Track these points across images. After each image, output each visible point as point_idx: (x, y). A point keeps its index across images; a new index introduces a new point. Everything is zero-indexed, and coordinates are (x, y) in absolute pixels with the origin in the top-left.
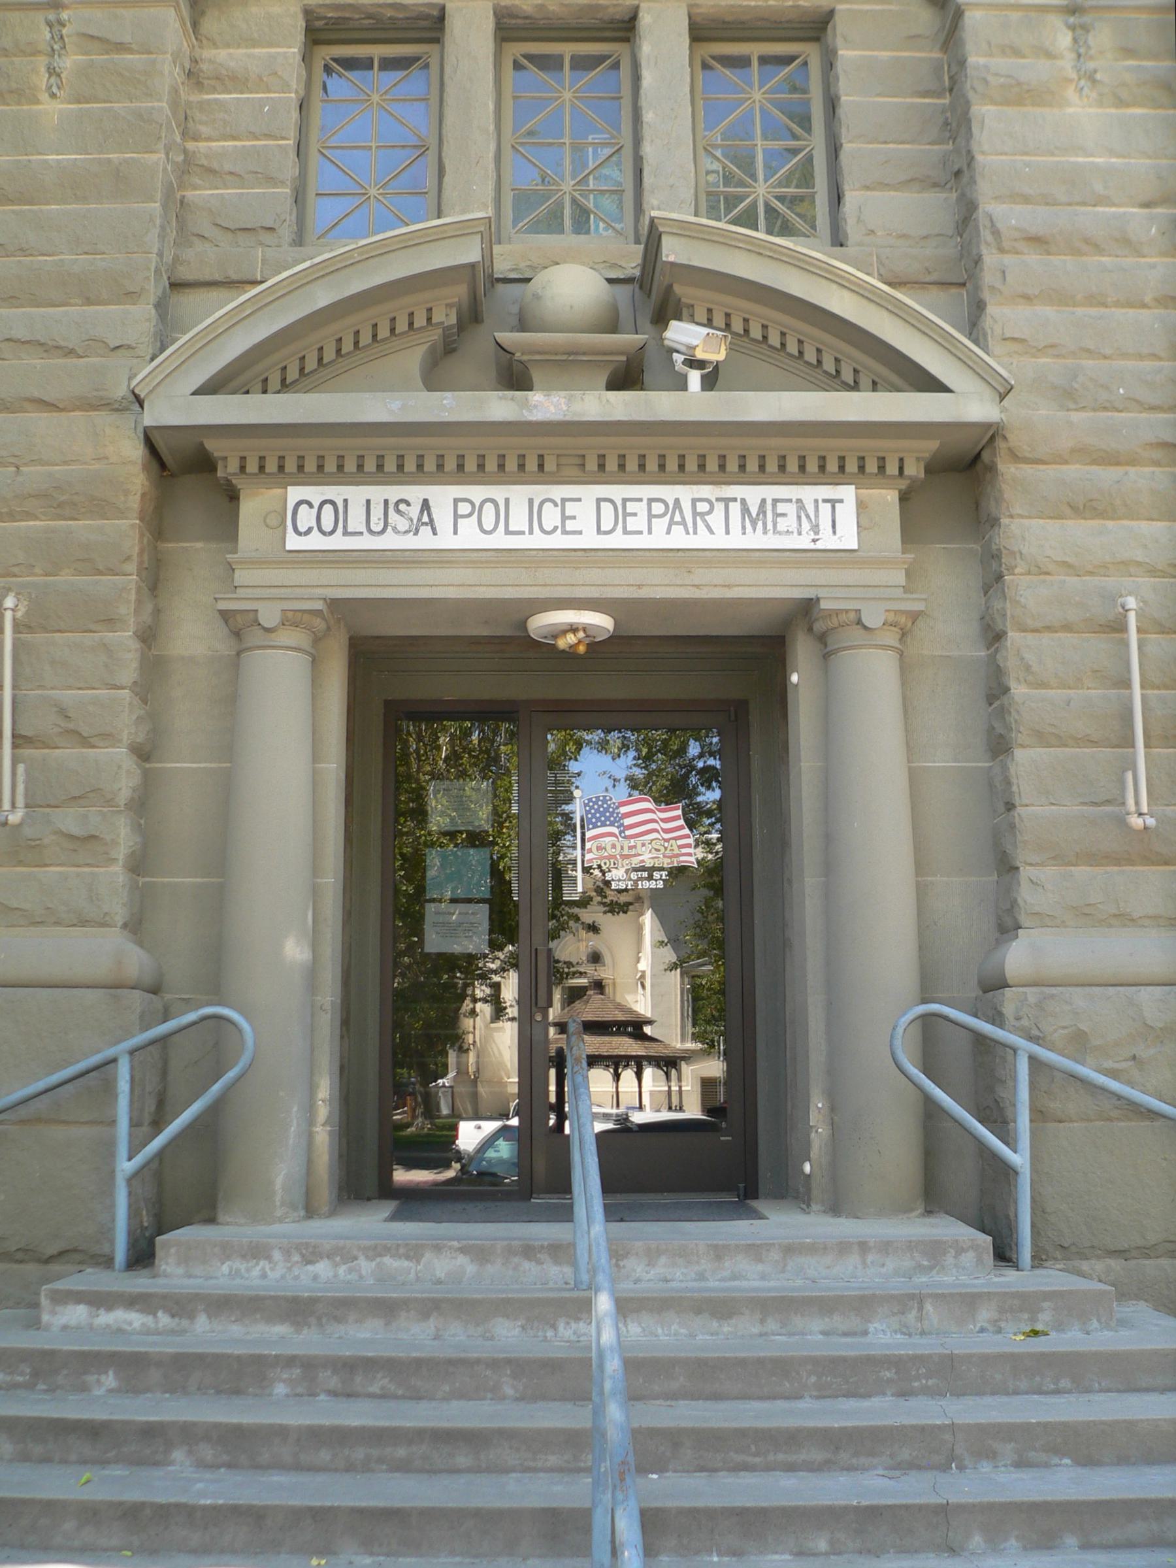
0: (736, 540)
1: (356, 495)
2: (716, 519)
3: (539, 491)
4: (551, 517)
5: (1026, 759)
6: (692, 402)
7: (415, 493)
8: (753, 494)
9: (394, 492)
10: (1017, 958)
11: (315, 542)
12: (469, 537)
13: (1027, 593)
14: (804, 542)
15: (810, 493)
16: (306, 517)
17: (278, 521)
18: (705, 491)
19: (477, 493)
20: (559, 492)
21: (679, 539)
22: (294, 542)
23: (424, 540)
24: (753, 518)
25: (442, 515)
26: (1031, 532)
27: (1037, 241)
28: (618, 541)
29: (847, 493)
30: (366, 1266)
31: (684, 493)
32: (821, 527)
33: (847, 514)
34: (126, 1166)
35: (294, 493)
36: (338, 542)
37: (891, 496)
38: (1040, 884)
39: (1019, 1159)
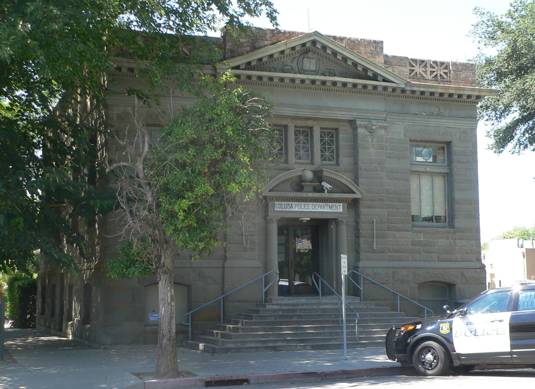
0: (328, 210)
1: (283, 203)
2: (326, 207)
3: (305, 203)
4: (307, 207)
5: (362, 240)
6: (326, 195)
7: (290, 203)
8: (330, 204)
9: (288, 203)
10: (361, 264)
11: (278, 209)
12: (297, 209)
13: (363, 218)
14: (336, 211)
15: (337, 204)
16: (277, 206)
17: (274, 205)
18: (325, 204)
19: (298, 203)
20: (308, 203)
21: (321, 210)
22: (276, 209)
23: (291, 210)
24: (331, 207)
25: (294, 206)
26: (363, 210)
27: (366, 170)
28: (314, 210)
29: (341, 204)
30: (295, 301)
31: (322, 204)
32: (337, 209)
33: (341, 207)
34: (264, 290)
35: (276, 203)
36: (281, 209)
37: (346, 204)
38: (363, 255)
39: (361, 289)
